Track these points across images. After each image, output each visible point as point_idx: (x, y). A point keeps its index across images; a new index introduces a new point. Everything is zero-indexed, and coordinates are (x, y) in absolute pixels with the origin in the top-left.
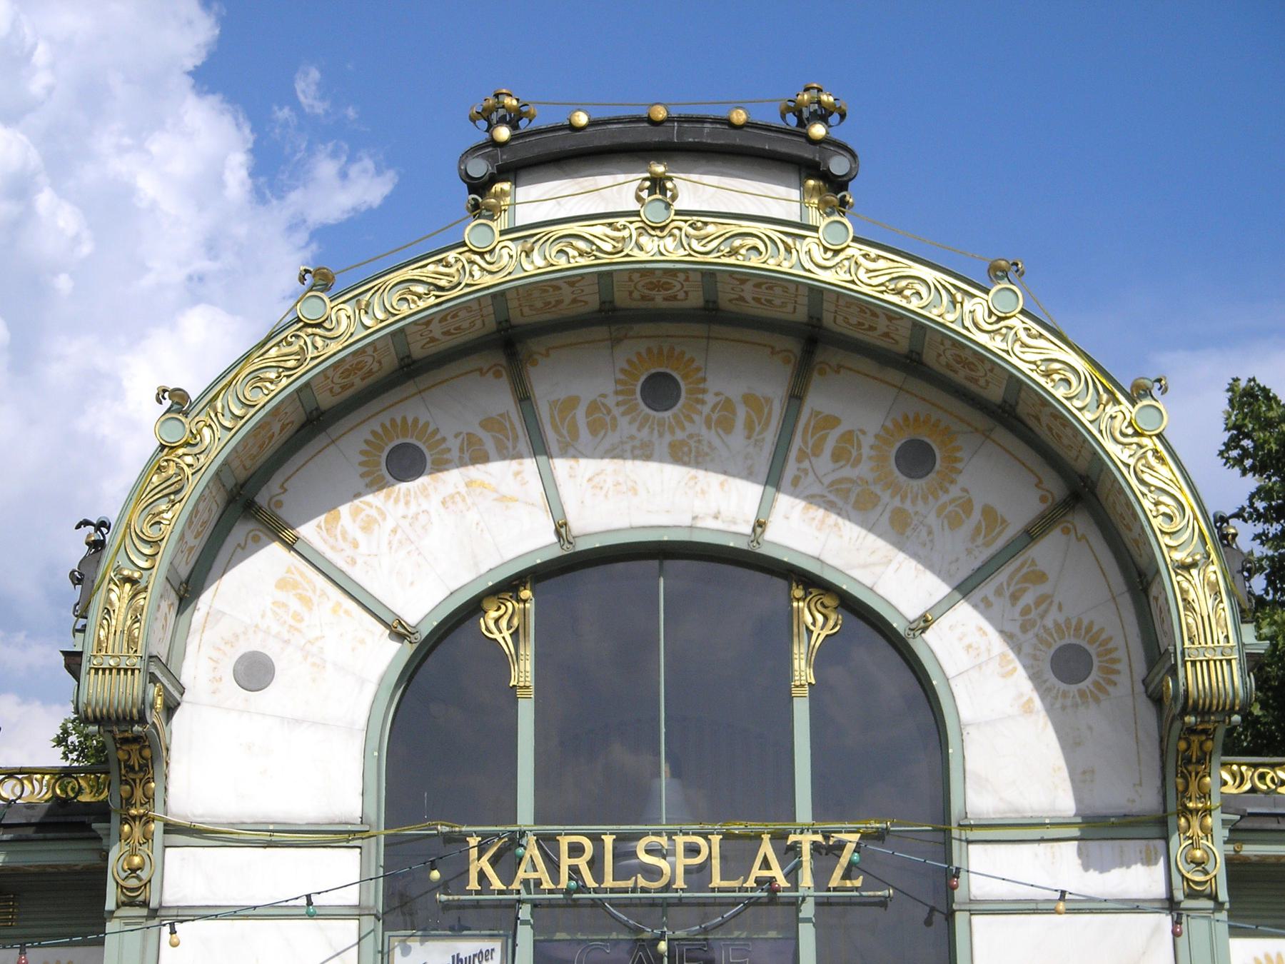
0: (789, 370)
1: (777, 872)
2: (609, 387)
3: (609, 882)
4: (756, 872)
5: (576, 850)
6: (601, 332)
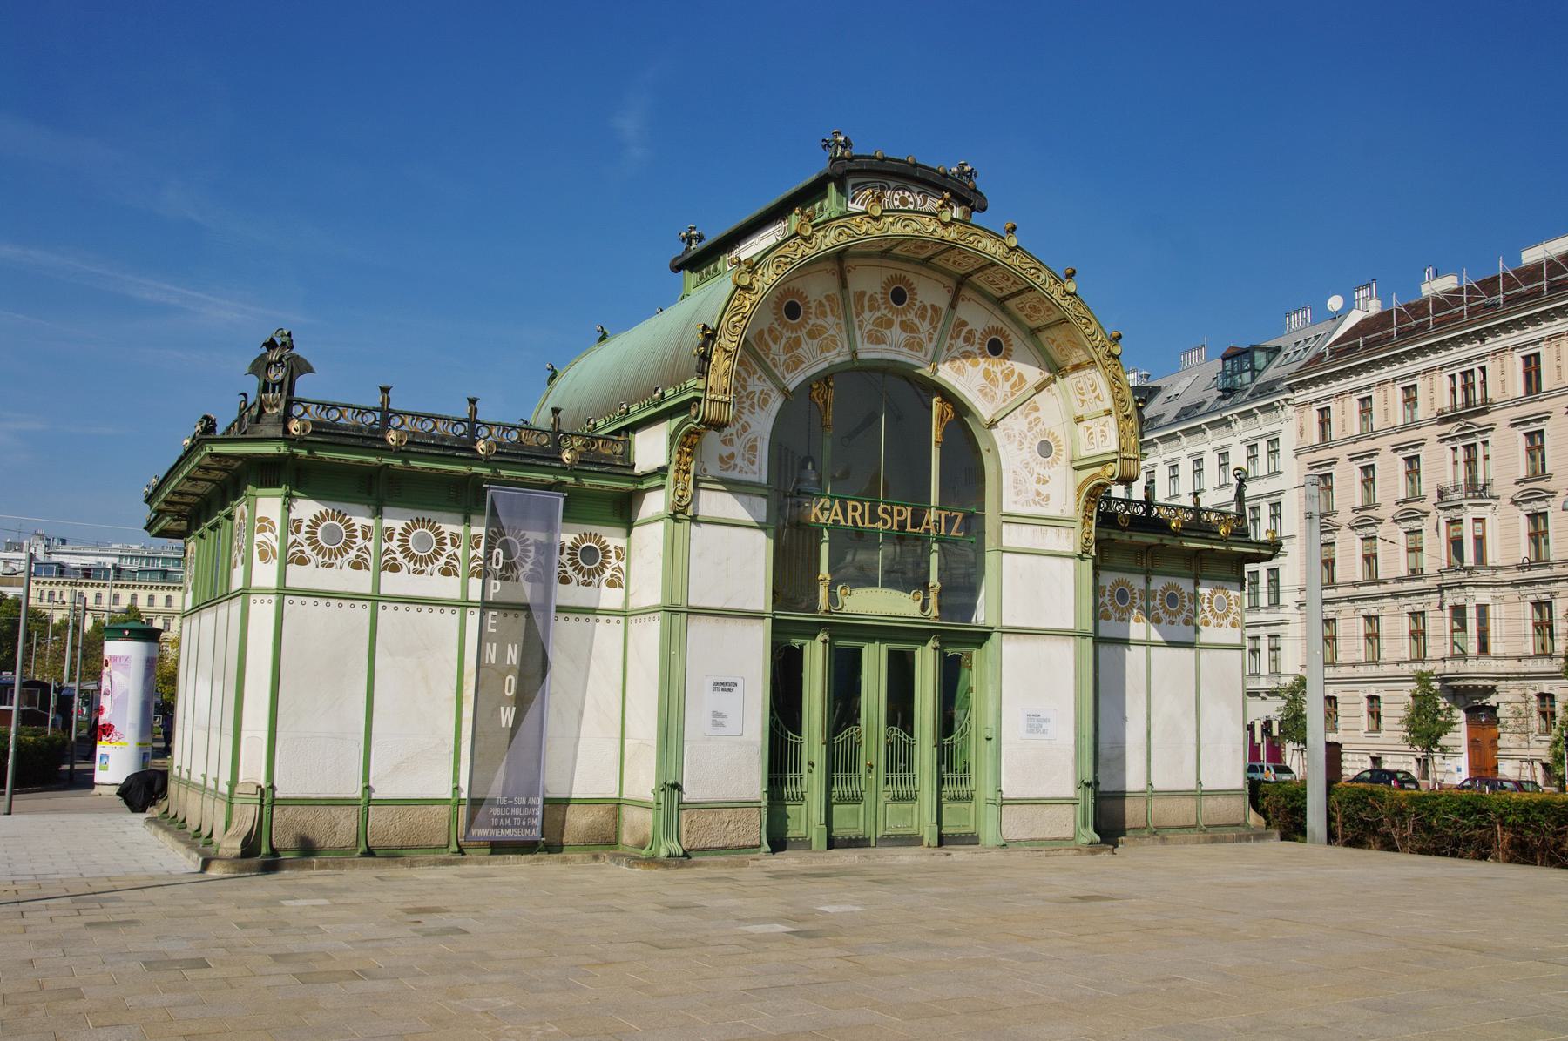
2: (878, 290)
3: (867, 524)
5: (855, 509)
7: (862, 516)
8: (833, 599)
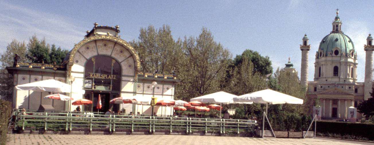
0: (114, 45)
1: (110, 77)
4: (109, 77)
6: (102, 41)
7: (99, 76)
8: (95, 88)
